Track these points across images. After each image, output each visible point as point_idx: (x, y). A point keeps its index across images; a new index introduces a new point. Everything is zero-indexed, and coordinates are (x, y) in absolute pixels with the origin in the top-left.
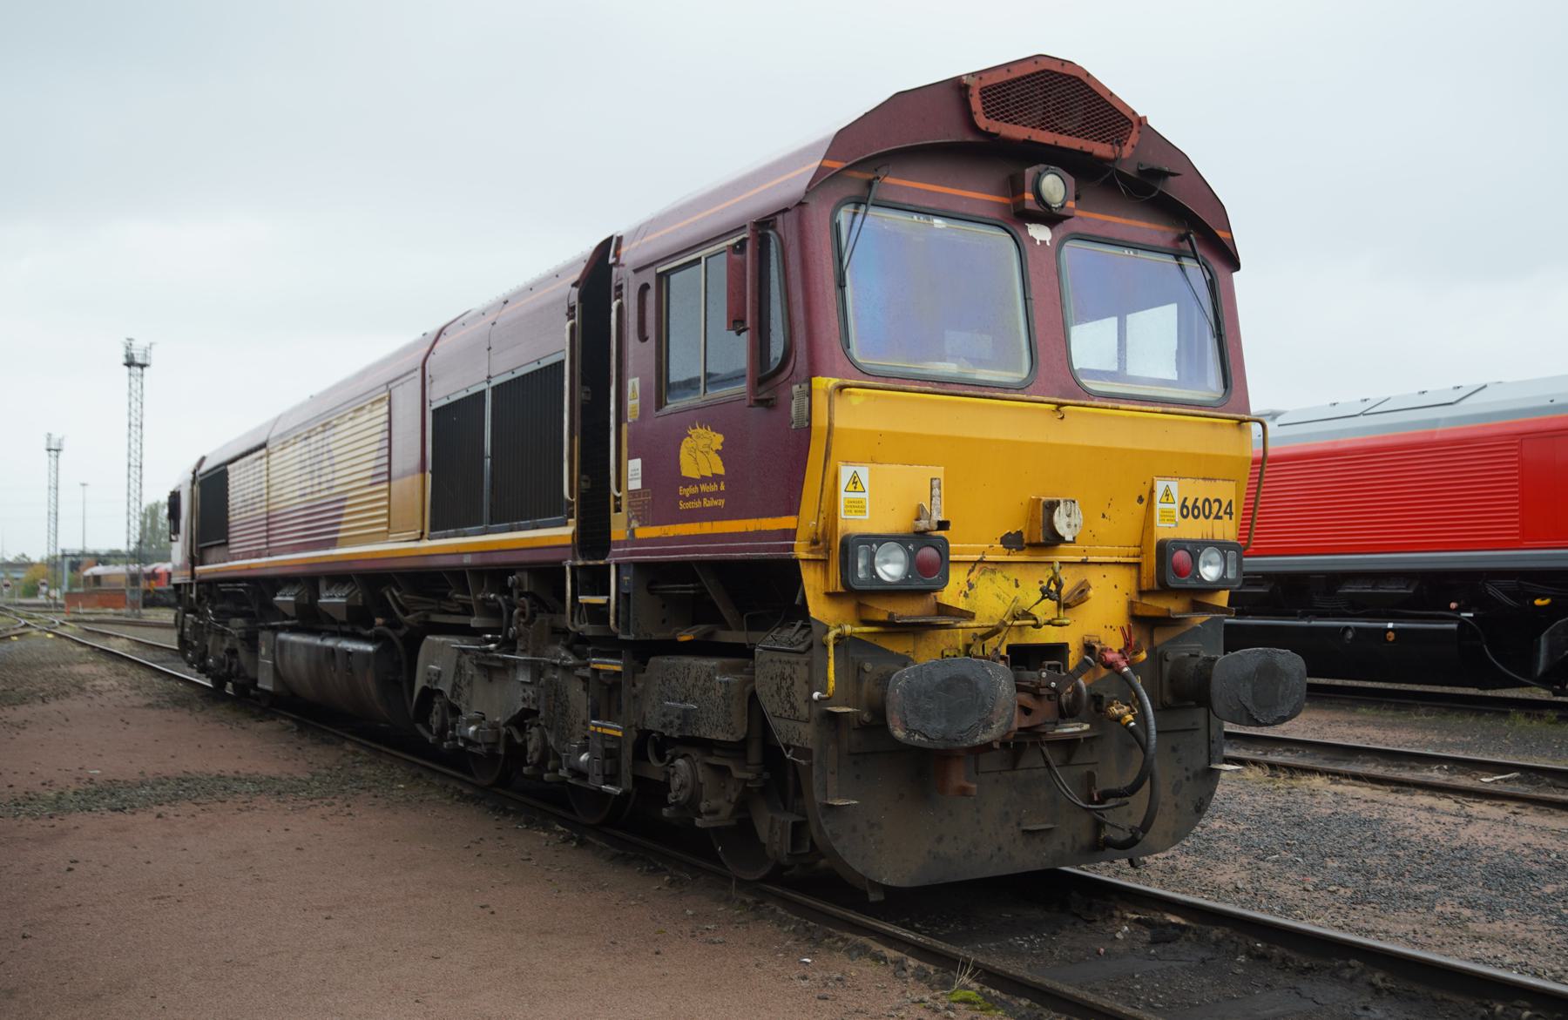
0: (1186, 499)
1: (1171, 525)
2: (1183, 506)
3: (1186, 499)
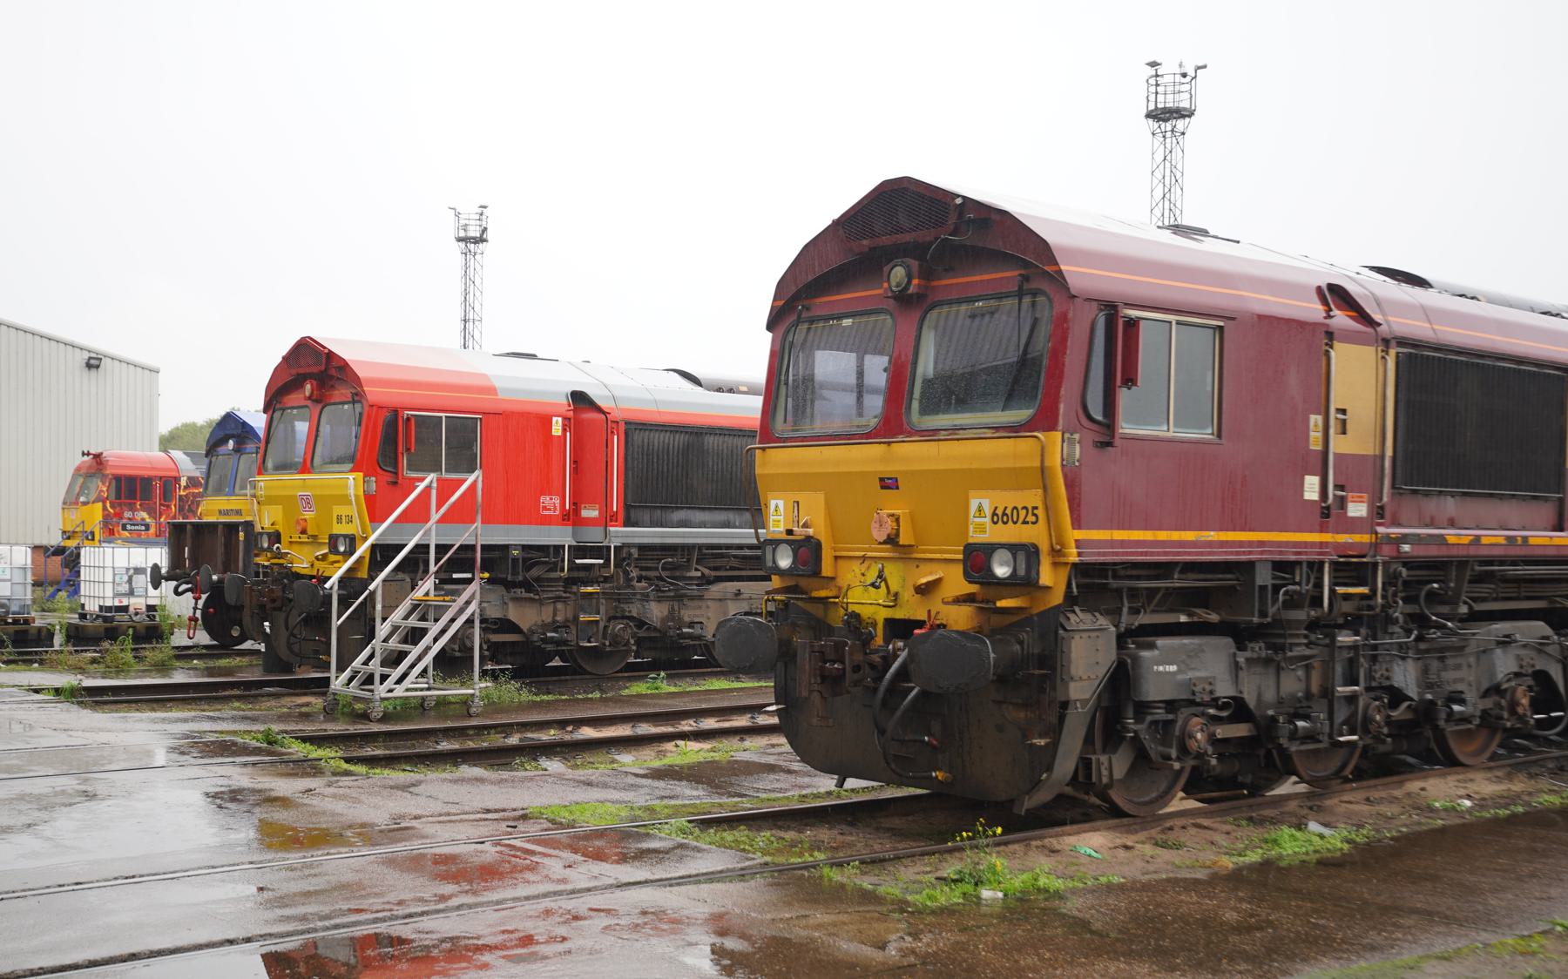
0: (996, 508)
1: (983, 531)
2: (994, 514)
3: (996, 508)
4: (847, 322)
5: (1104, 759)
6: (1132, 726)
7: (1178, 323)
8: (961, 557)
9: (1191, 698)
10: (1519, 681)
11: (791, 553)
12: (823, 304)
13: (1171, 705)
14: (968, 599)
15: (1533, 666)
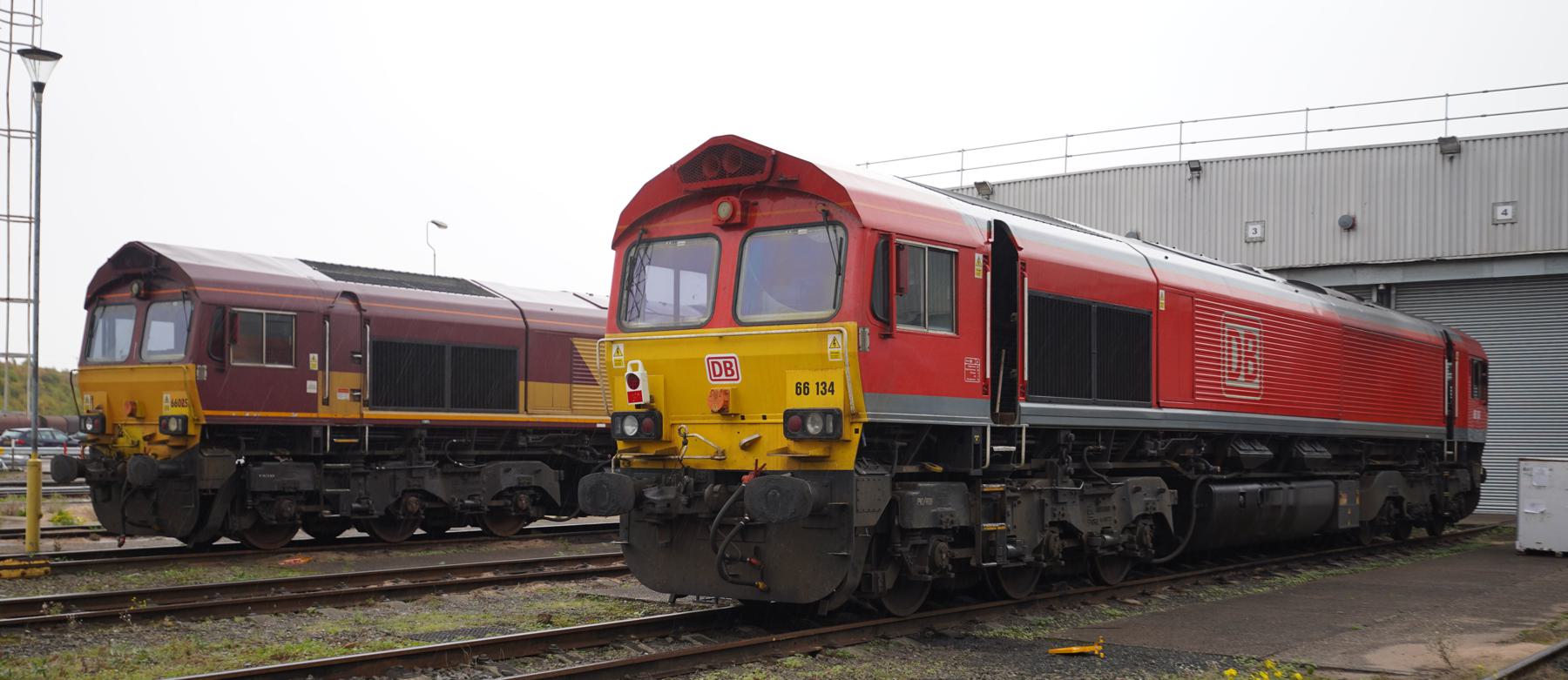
4: (681, 243)
5: (879, 573)
6: (900, 549)
7: (929, 248)
8: (782, 421)
9: (939, 526)
10: (1145, 521)
11: (637, 424)
12: (662, 226)
13: (927, 532)
14: (784, 451)
15: (1154, 509)
